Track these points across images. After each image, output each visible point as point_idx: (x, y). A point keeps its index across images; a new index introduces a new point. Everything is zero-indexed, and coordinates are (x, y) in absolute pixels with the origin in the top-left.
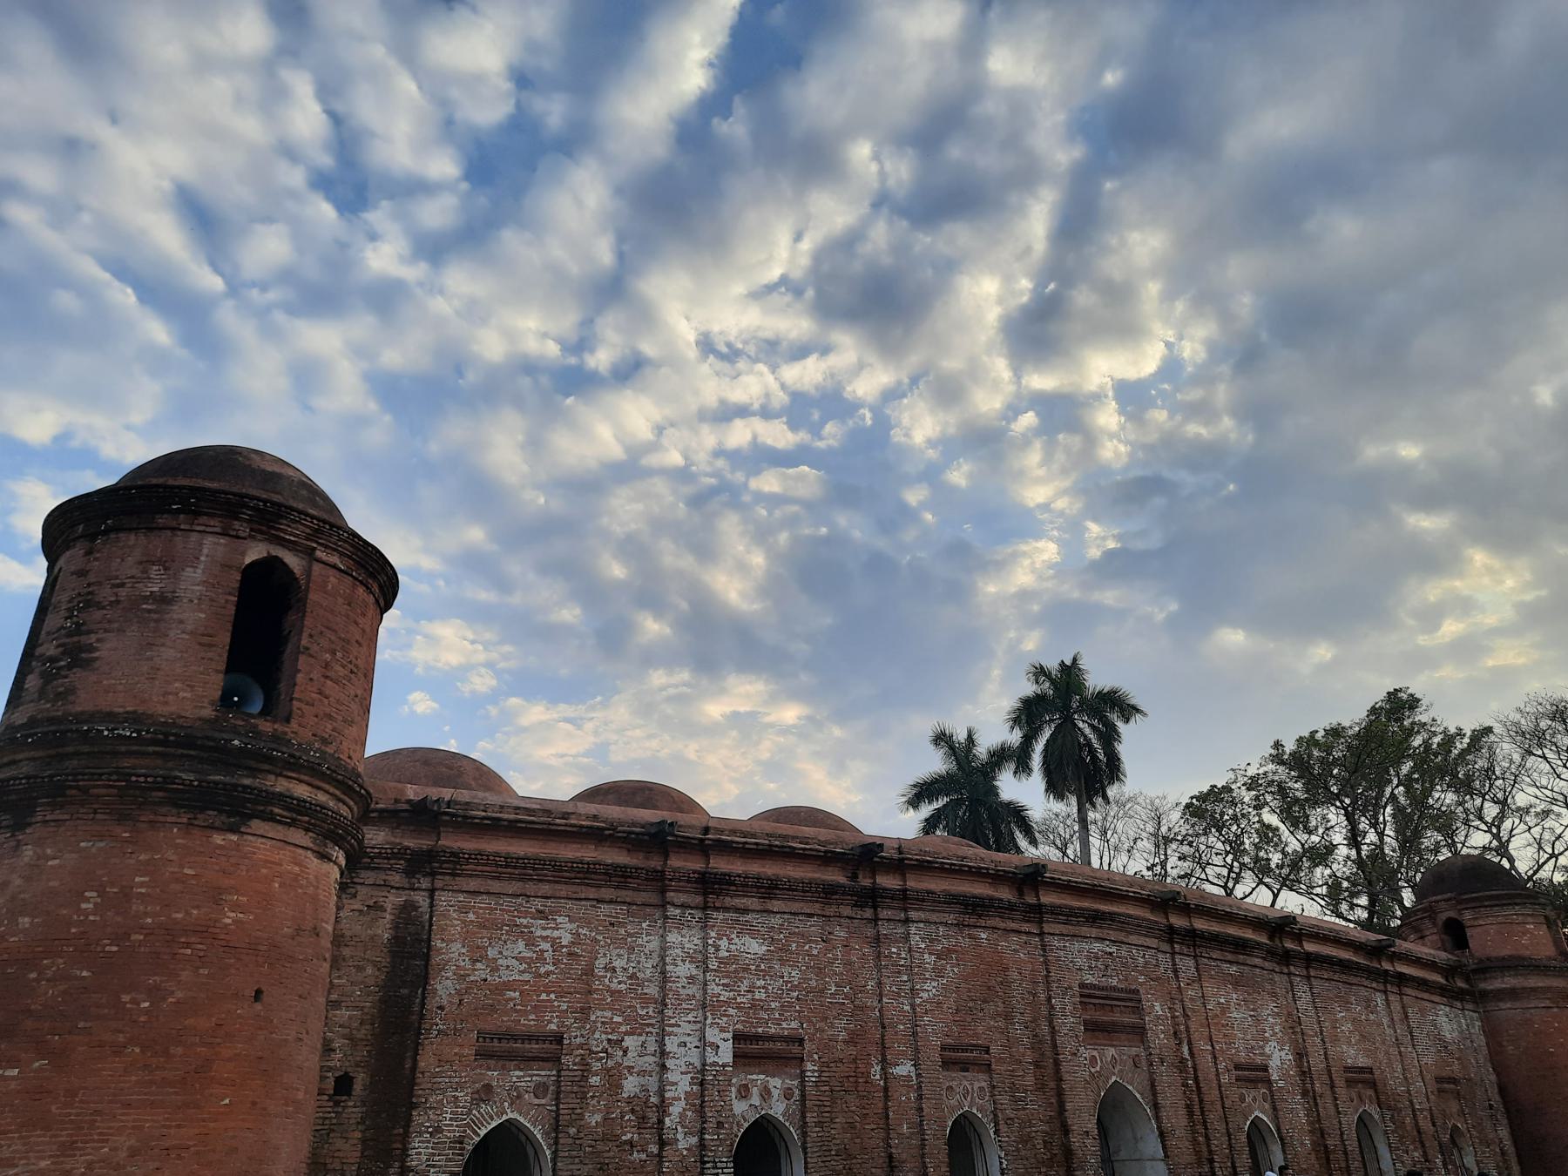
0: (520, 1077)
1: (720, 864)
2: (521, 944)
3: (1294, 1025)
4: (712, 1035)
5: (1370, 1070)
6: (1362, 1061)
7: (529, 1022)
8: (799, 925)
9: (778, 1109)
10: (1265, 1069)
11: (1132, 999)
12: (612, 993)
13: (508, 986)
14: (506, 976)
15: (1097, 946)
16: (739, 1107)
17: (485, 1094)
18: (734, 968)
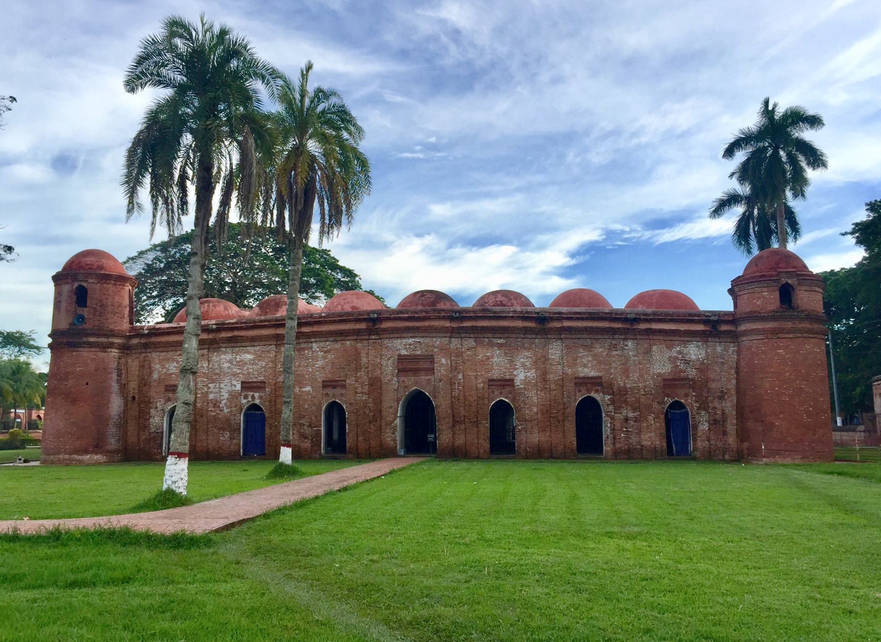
1: (236, 333)
2: (175, 364)
3: (542, 363)
4: (234, 382)
5: (600, 378)
6: (593, 374)
9: (257, 402)
10: (512, 380)
11: (431, 359)
12: (204, 373)
13: (171, 374)
14: (171, 371)
15: (411, 341)
16: (244, 401)
18: (241, 364)
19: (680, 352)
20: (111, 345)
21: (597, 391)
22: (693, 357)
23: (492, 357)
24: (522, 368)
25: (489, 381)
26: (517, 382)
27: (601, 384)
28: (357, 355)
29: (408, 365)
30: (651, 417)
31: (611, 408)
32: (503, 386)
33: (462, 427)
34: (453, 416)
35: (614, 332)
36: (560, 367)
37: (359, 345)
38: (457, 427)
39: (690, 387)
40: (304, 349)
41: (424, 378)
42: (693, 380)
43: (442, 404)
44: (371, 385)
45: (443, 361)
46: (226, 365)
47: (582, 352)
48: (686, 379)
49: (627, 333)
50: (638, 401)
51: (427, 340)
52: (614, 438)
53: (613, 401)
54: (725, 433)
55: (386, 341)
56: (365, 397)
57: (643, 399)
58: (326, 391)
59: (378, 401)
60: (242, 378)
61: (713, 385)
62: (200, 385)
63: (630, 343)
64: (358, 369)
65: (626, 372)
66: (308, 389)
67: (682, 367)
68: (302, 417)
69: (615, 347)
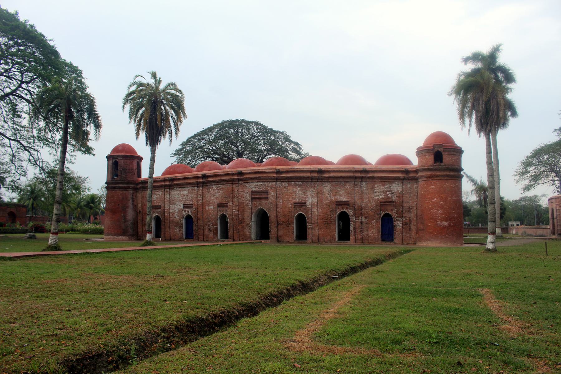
0: (158, 210)
5: (348, 202)
6: (344, 199)
7: (157, 204)
8: (193, 188)
9: (190, 213)
10: (305, 203)
11: (266, 193)
15: (257, 184)
16: (184, 213)
17: (154, 212)
18: (183, 196)
19: (389, 188)
20: (129, 188)
21: (347, 208)
22: (396, 190)
23: (296, 191)
24: (309, 197)
25: (295, 203)
26: (308, 204)
27: (348, 205)
28: (233, 190)
29: (257, 196)
30: (373, 222)
31: (354, 217)
32: (301, 206)
33: (282, 226)
34: (277, 221)
35: (355, 178)
36: (329, 196)
37: (234, 186)
38: (279, 226)
39: (394, 206)
40: (209, 188)
41: (264, 202)
42: (395, 202)
43: (272, 215)
44: (239, 206)
45: (273, 193)
46: (177, 196)
47: (339, 188)
48: (392, 202)
49: (362, 179)
50: (367, 213)
51: (265, 183)
52: (355, 232)
53: (355, 214)
54: (410, 229)
55: (246, 184)
56: (237, 212)
57: (370, 212)
58: (219, 209)
59: (243, 213)
60: (183, 202)
61: (405, 205)
62: (166, 205)
63: (364, 183)
64: (233, 198)
65: (362, 198)
66: (211, 207)
67: (390, 195)
68: (209, 221)
69: (355, 185)
